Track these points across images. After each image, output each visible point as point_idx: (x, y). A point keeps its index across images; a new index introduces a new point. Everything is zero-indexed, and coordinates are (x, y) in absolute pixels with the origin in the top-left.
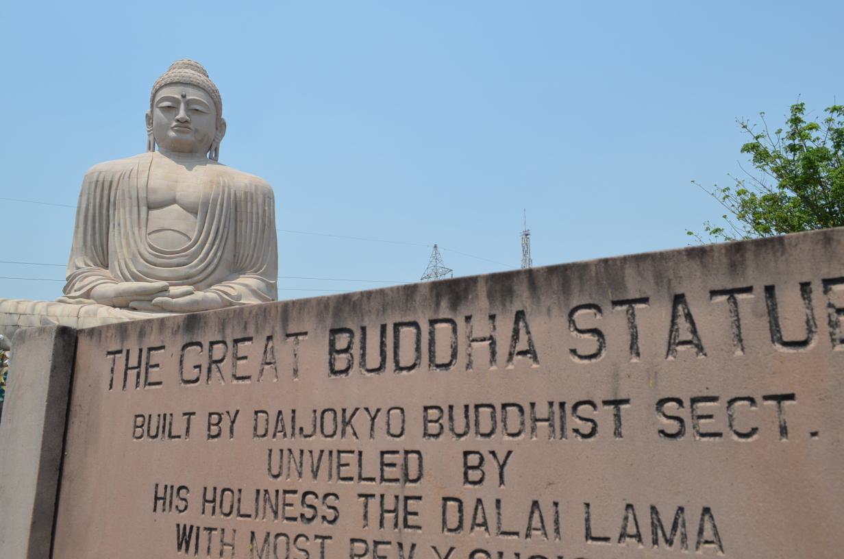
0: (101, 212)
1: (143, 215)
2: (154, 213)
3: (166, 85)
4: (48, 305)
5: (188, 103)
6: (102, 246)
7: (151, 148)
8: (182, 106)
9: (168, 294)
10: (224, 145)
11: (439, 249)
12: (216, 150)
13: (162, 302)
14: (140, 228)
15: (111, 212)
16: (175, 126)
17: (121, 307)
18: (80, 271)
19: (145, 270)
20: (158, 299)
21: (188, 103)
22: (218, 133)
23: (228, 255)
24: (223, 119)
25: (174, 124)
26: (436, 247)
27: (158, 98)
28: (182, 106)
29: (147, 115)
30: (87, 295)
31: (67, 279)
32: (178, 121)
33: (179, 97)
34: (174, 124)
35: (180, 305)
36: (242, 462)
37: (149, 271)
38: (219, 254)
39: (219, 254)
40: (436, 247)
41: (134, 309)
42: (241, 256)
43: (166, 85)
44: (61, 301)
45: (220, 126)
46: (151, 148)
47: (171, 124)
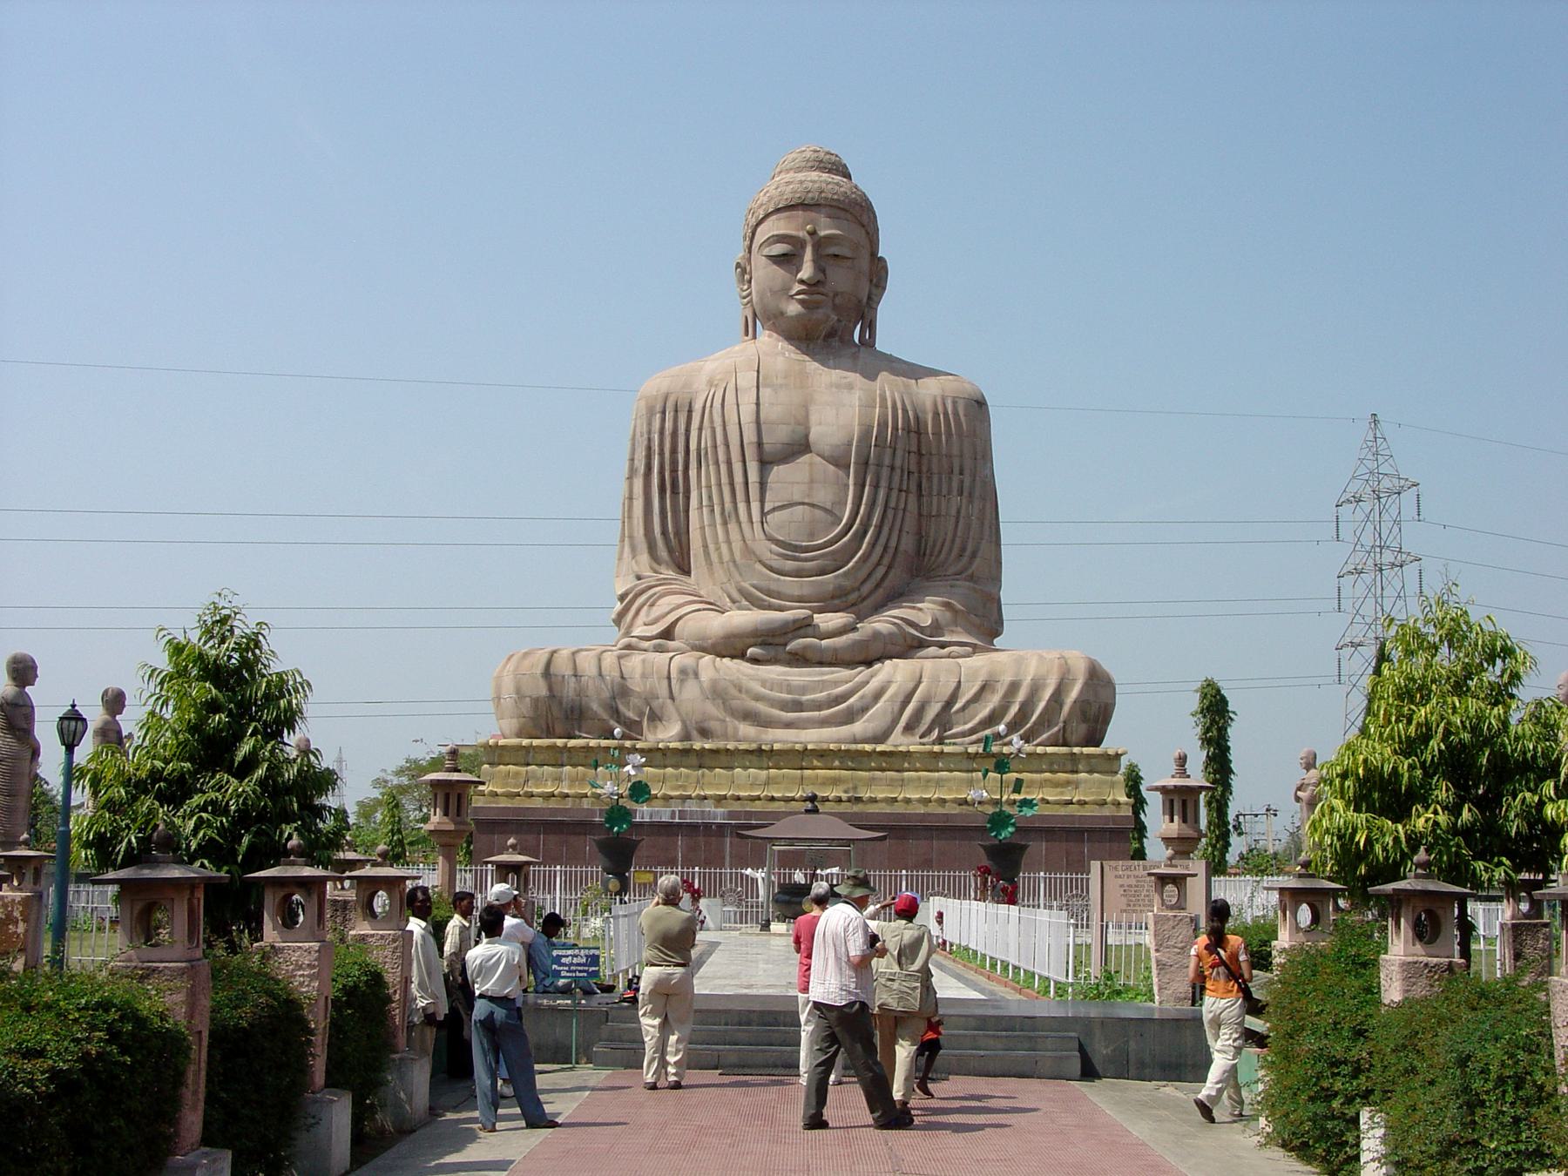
0: (674, 470)
1: (753, 477)
2: (778, 472)
3: (778, 211)
4: (620, 658)
5: (820, 244)
6: (677, 534)
7: (749, 331)
8: (808, 254)
9: (810, 630)
10: (886, 312)
11: (1382, 425)
12: (871, 326)
13: (806, 647)
14: (748, 501)
15: (693, 473)
16: (798, 293)
17: (733, 657)
18: (643, 584)
19: (763, 584)
20: (796, 644)
21: (820, 244)
22: (874, 291)
23: (908, 543)
24: (882, 260)
25: (798, 287)
26: (1375, 419)
27: (761, 237)
28: (808, 254)
29: (738, 265)
30: (667, 634)
31: (622, 598)
32: (802, 282)
33: (801, 234)
34: (798, 287)
35: (835, 650)
36: (1133, 881)
37: (773, 586)
38: (893, 544)
39: (893, 544)
40: (1375, 419)
41: (755, 661)
42: (930, 543)
43: (778, 211)
44: (629, 647)
45: (877, 274)
46: (749, 331)
47: (790, 288)
